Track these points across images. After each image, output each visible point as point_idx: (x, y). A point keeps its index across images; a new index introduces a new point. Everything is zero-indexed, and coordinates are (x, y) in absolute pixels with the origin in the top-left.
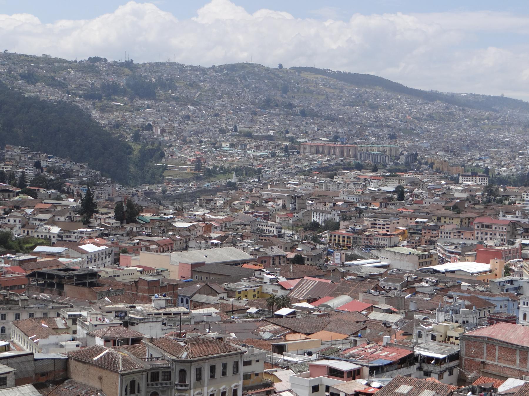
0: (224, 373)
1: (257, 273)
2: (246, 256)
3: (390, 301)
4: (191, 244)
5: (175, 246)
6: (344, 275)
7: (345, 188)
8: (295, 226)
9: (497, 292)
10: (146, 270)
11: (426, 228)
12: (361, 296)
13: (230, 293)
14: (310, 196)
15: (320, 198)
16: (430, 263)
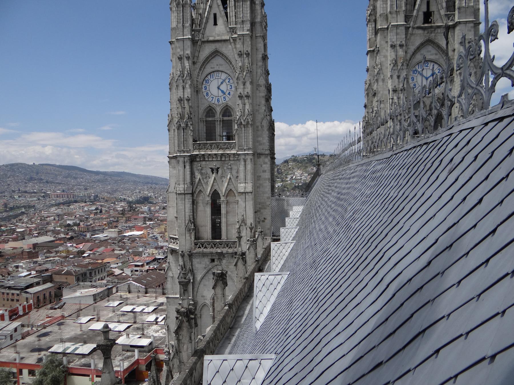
0: (102, 272)
1: (65, 244)
2: (52, 239)
3: (119, 247)
4: (26, 237)
5: (19, 238)
6: (95, 241)
7: (78, 209)
8: (60, 226)
9: (150, 239)
10: (14, 248)
11: (114, 222)
12: (109, 247)
13: (57, 252)
14: (65, 214)
15: (69, 214)
16: (122, 233)
